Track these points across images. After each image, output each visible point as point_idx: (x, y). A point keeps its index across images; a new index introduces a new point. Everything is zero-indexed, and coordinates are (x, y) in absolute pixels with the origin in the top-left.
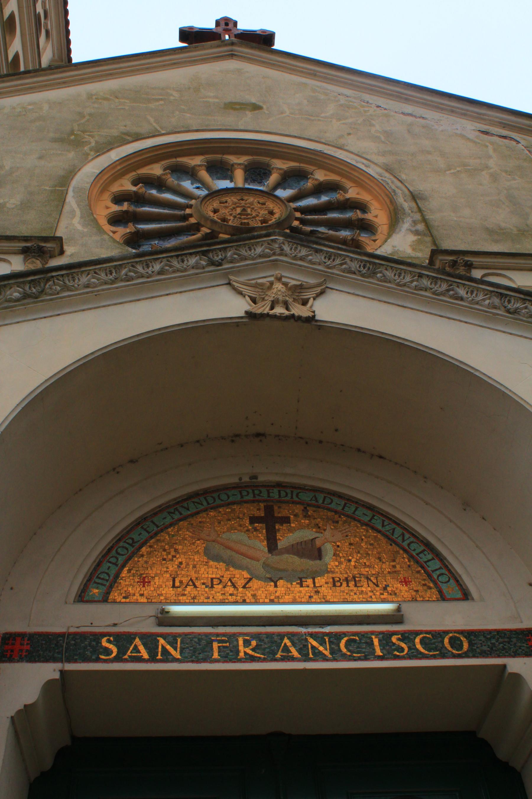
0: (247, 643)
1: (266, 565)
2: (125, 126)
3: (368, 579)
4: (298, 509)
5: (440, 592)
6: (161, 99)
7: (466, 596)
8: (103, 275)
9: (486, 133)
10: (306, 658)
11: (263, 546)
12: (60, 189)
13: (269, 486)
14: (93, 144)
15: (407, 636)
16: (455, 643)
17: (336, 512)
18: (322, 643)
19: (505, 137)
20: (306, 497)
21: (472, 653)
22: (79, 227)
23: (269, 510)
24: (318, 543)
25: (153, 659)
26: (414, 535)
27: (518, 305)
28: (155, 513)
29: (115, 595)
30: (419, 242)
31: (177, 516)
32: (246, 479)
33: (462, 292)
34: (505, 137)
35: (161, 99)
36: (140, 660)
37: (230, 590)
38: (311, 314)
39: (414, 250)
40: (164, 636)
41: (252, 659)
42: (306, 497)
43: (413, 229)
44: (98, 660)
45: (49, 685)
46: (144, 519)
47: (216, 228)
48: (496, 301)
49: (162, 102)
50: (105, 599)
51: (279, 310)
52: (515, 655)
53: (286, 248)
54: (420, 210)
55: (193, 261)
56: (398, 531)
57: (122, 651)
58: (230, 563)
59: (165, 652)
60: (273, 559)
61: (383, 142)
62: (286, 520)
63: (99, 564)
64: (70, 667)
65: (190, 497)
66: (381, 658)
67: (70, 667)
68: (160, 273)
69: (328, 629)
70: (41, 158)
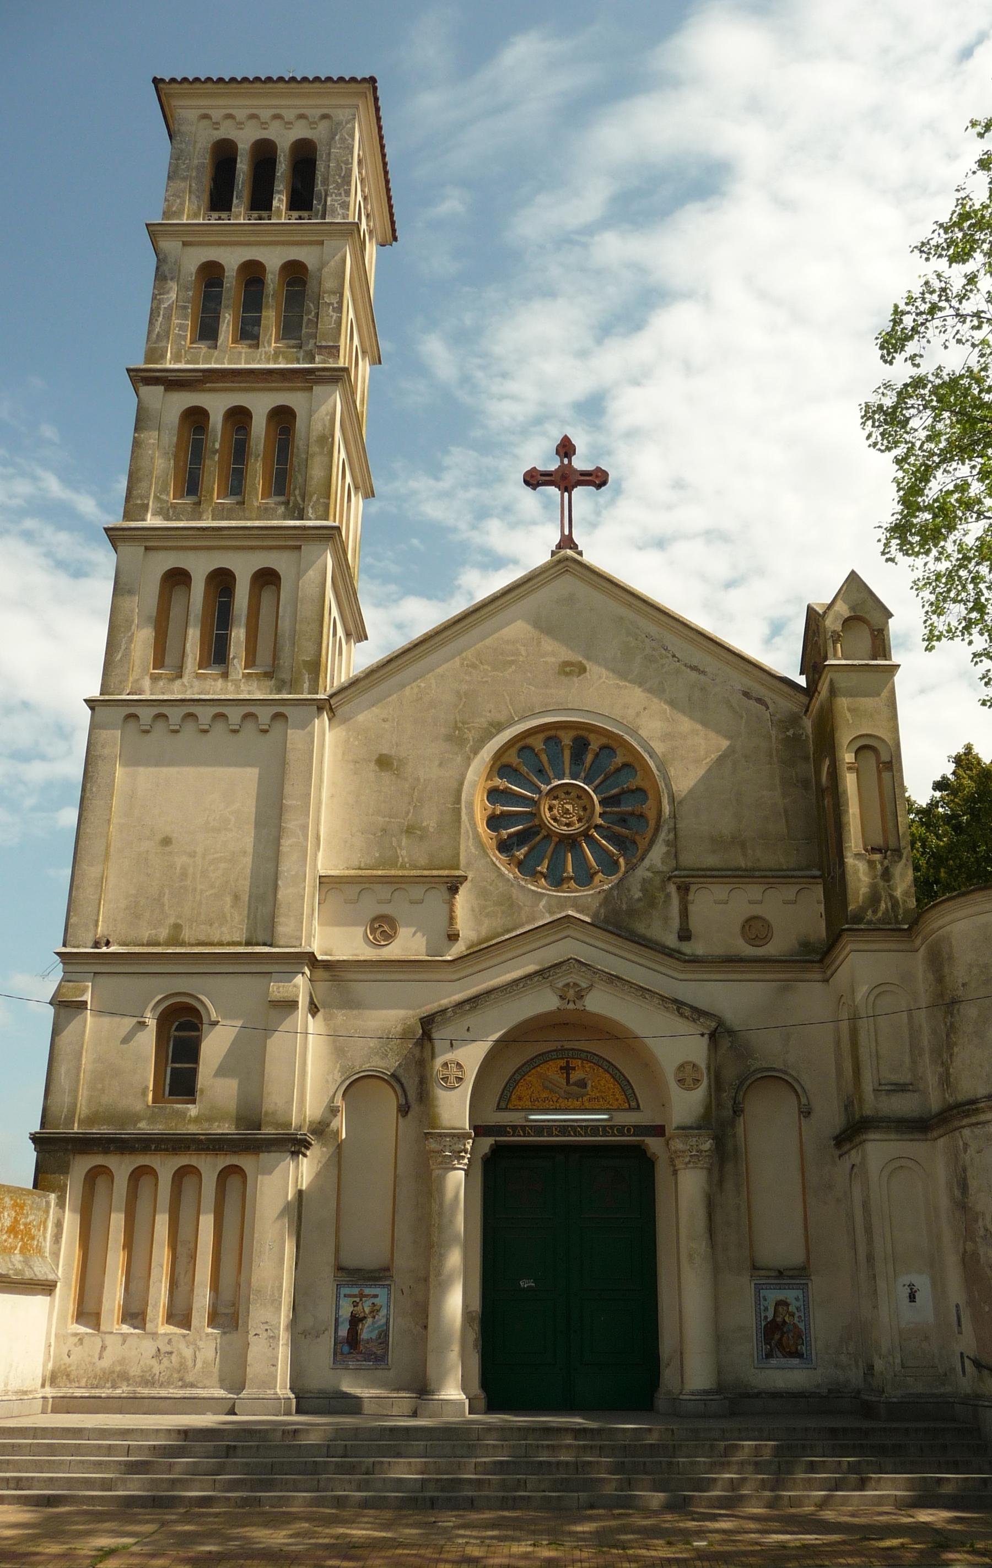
0: (556, 1129)
1: (565, 1091)
2: (490, 711)
3: (603, 1098)
4: (580, 1062)
5: (629, 1105)
6: (513, 662)
7: (638, 1108)
8: (500, 994)
9: (746, 694)
10: (576, 1136)
11: (564, 1082)
12: (456, 806)
13: (567, 1049)
14: (471, 743)
15: (612, 1127)
16: (629, 1130)
17: (594, 1063)
18: (582, 1129)
19: (759, 700)
20: (584, 1055)
21: (634, 1135)
22: (473, 851)
23: (568, 1062)
24: (586, 1080)
25: (524, 1136)
26: (624, 1076)
27: (670, 1005)
28: (523, 1065)
29: (510, 1106)
30: (668, 853)
31: (532, 1066)
32: (559, 1047)
33: (647, 996)
34: (759, 700)
35: (513, 662)
36: (520, 1136)
37: (551, 1103)
38: (583, 1008)
39: (662, 863)
40: (528, 1126)
41: (558, 1136)
42: (584, 1055)
43: (667, 839)
44: (506, 1136)
45: (492, 1145)
46: (519, 1068)
47: (550, 833)
48: (661, 1003)
49: (513, 667)
50: (506, 1109)
51: (571, 1006)
52: (649, 1136)
53: (576, 966)
54: (675, 817)
55: (536, 979)
56: (618, 1074)
57: (514, 1133)
58: (552, 1091)
59: (529, 1133)
60: (568, 1088)
61: (668, 718)
62: (574, 1069)
63: (503, 1092)
64: (497, 1139)
65: (536, 1057)
66: (601, 1136)
67: (497, 1139)
68: (523, 987)
69: (584, 1124)
70: (440, 765)
